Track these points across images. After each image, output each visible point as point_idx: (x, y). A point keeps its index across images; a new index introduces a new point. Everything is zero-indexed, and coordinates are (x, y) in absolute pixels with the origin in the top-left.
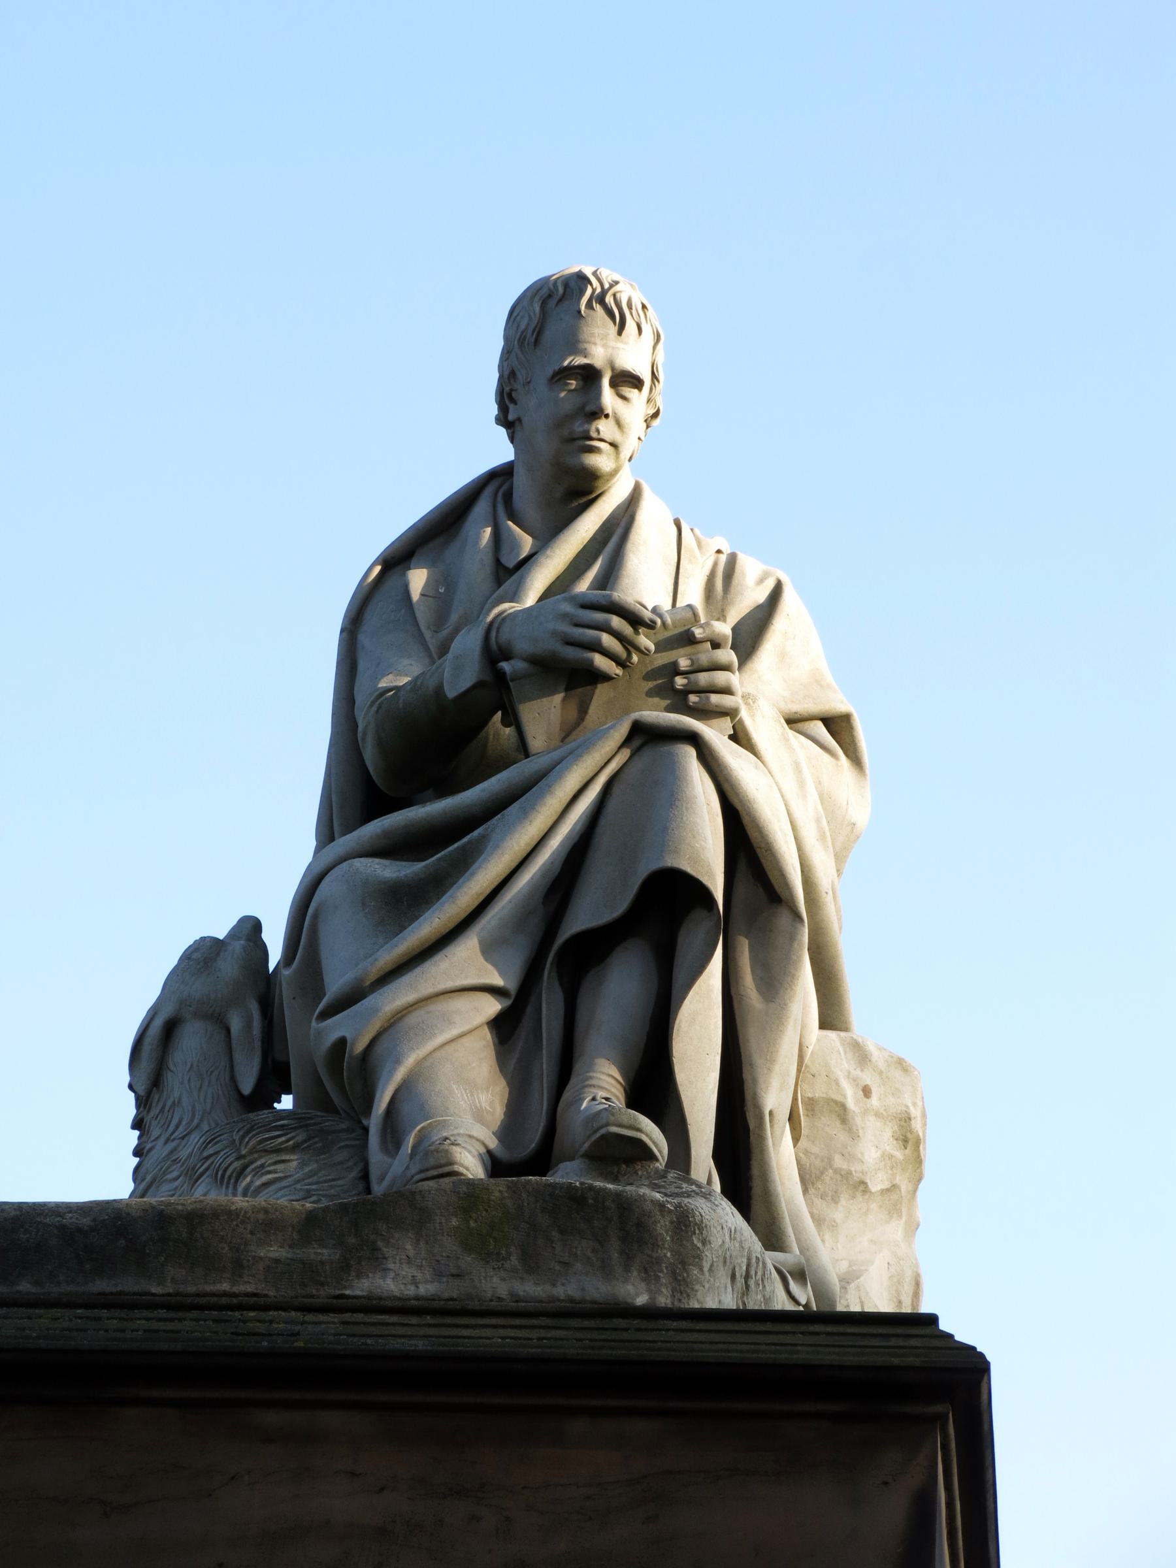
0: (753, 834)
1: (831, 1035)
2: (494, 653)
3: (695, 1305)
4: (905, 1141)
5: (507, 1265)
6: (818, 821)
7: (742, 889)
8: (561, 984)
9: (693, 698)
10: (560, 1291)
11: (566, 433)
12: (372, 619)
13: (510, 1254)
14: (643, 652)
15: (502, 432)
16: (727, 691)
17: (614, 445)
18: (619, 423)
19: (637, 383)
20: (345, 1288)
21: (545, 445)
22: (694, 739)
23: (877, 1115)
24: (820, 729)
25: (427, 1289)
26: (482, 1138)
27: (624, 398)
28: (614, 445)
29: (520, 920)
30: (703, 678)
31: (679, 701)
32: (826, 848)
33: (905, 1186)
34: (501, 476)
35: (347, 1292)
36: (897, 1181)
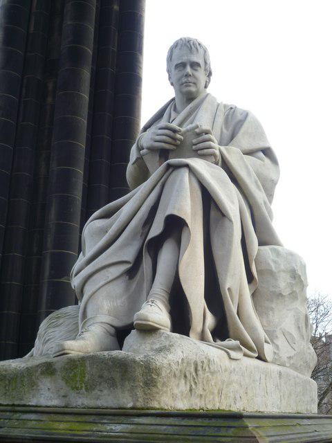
0: (212, 194)
1: (267, 248)
3: (156, 405)
4: (295, 278)
5: (81, 391)
6: (256, 182)
7: (213, 213)
8: (150, 256)
9: (199, 152)
10: (99, 403)
11: (180, 82)
13: (82, 387)
14: (180, 140)
15: (172, 87)
17: (194, 83)
18: (195, 77)
19: (198, 65)
20: (30, 402)
22: (187, 166)
23: (284, 271)
24: (261, 154)
25: (55, 402)
26: (110, 323)
27: (196, 70)
28: (194, 83)
29: (133, 236)
32: (260, 190)
33: (297, 289)
35: (30, 403)
36: (294, 289)
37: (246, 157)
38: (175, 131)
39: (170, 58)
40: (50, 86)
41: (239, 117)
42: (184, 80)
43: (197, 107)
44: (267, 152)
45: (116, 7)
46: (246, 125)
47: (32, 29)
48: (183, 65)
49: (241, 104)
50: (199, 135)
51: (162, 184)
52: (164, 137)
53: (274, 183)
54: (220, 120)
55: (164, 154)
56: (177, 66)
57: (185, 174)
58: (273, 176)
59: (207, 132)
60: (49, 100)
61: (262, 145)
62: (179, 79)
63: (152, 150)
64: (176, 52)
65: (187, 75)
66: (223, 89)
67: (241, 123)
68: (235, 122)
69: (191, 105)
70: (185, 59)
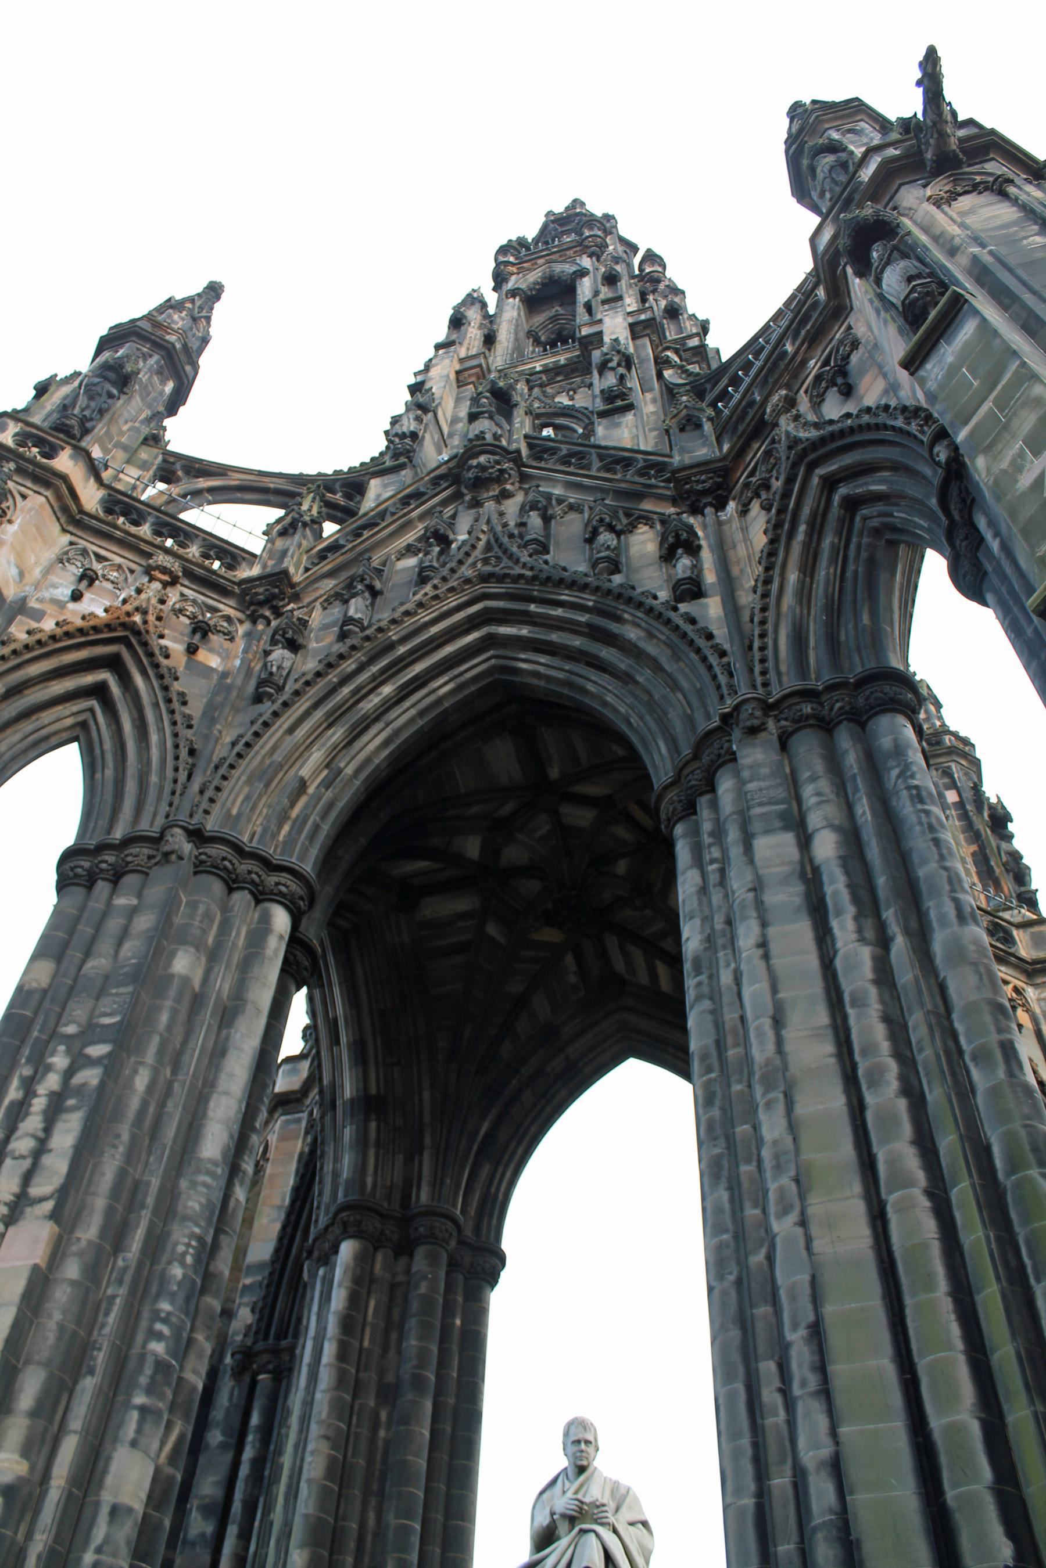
2: (552, 1514)
12: (537, 1507)
16: (607, 1517)
19: (590, 1442)
21: (572, 1459)
22: (594, 1531)
24: (640, 1526)
30: (601, 1515)
31: (596, 1521)
34: (566, 1469)
37: (631, 1528)
38: (582, 1502)
39: (566, 1434)
40: (383, 1416)
41: (623, 1491)
42: (578, 1454)
43: (587, 1479)
44: (645, 1524)
45: (458, 1322)
46: (628, 1499)
47: (366, 1344)
48: (578, 1442)
49: (625, 1481)
50: (598, 1507)
51: (575, 1544)
52: (574, 1507)
53: (650, 1552)
54: (607, 1493)
55: (572, 1520)
56: (574, 1442)
57: (592, 1535)
58: (650, 1546)
59: (604, 1505)
60: (382, 1433)
61: (642, 1518)
62: (574, 1454)
63: (563, 1516)
64: (573, 1429)
65: (582, 1451)
66: (606, 1464)
67: (624, 1497)
68: (621, 1496)
69: (582, 1478)
70: (580, 1436)
